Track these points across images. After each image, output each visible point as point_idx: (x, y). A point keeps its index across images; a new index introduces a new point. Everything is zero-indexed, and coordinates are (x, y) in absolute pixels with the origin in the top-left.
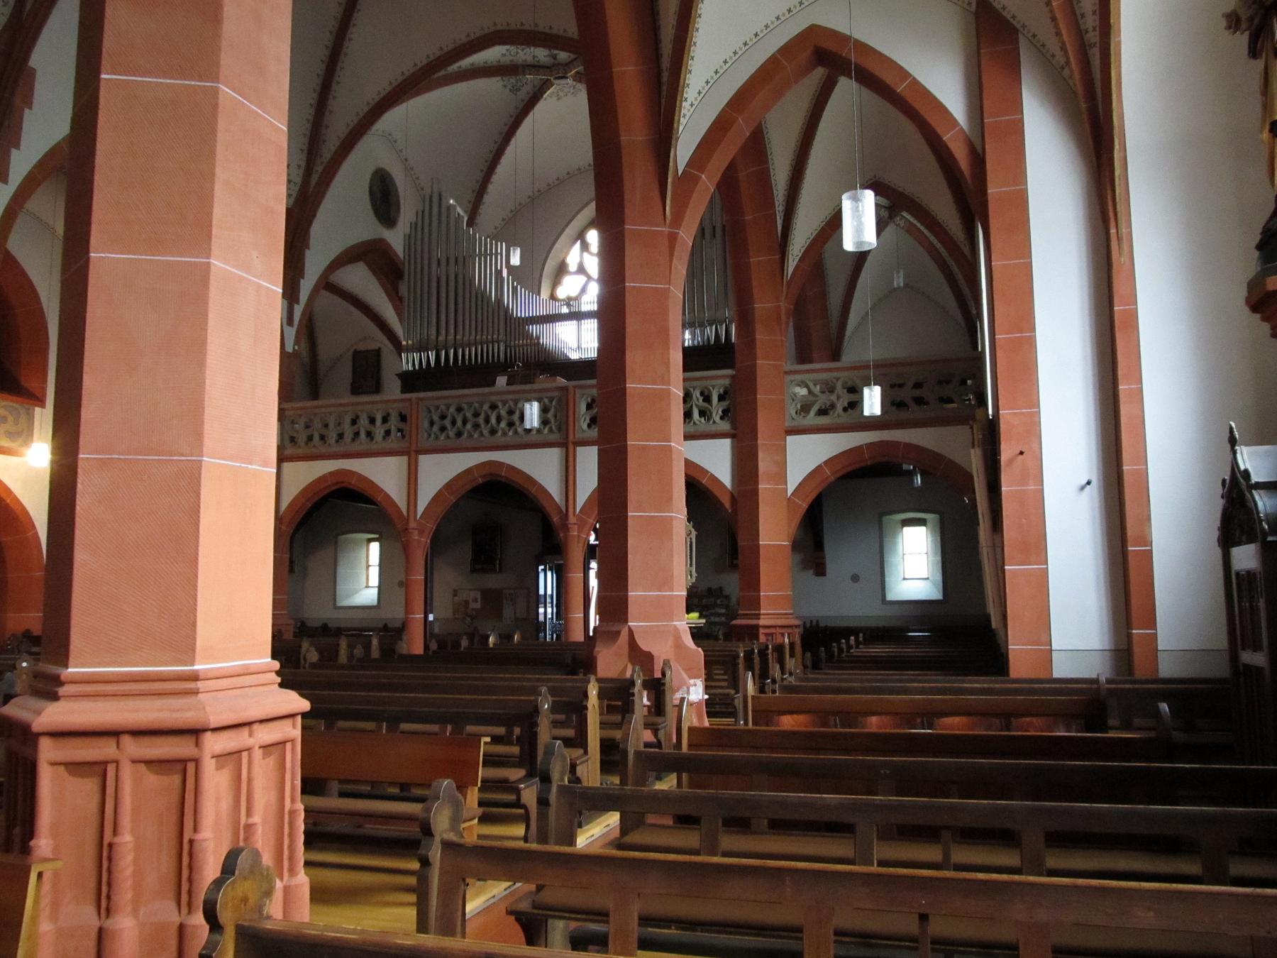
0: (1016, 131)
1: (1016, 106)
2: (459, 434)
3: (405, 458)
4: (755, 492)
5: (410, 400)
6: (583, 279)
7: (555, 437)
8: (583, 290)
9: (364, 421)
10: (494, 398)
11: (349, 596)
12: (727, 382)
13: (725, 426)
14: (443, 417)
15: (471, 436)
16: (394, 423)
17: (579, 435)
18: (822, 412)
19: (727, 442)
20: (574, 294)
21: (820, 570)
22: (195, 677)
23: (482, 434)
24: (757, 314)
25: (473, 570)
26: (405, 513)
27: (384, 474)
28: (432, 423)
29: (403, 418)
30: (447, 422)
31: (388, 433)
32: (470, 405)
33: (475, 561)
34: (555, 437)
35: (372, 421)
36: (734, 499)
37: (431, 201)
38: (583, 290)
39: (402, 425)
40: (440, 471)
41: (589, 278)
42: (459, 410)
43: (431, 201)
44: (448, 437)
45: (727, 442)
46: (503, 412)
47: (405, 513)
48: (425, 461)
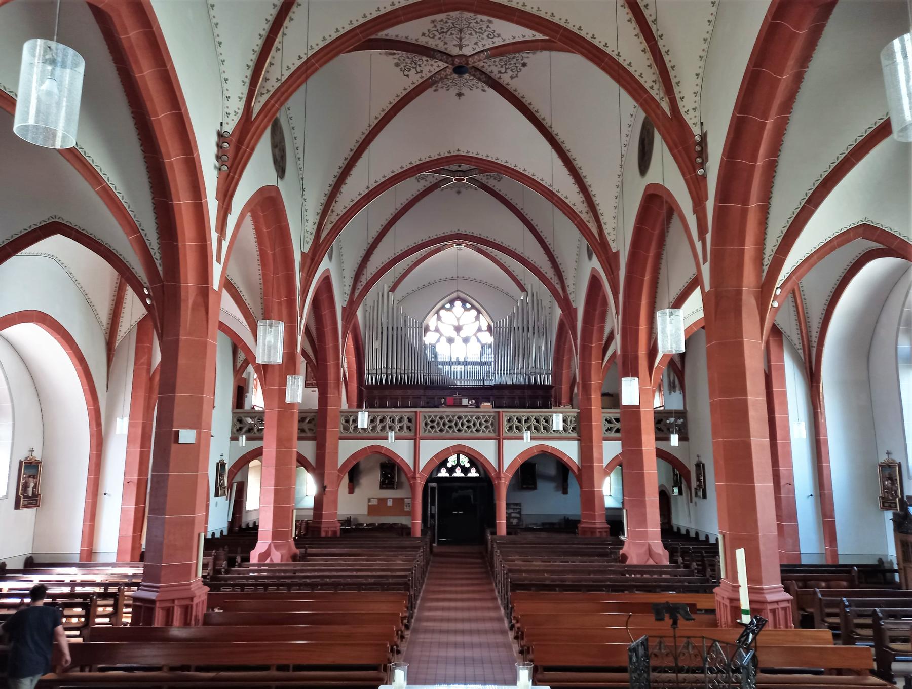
0: (782, 369)
1: (782, 360)
2: (441, 430)
3: (413, 441)
4: (592, 467)
5: (416, 412)
6: (437, 335)
7: (493, 435)
8: (438, 341)
9: (388, 420)
10: (460, 414)
11: (299, 502)
12: (575, 415)
13: (574, 435)
14: (432, 421)
15: (448, 431)
16: (405, 422)
17: (504, 435)
18: (618, 431)
19: (575, 443)
20: (433, 342)
21: (565, 492)
22: (762, 589)
23: (454, 431)
24: (593, 387)
25: (381, 488)
26: (412, 467)
27: (401, 449)
28: (426, 424)
29: (410, 420)
30: (435, 424)
31: (401, 428)
32: (448, 416)
33: (382, 483)
34: (493, 435)
35: (393, 421)
36: (579, 469)
37: (383, 296)
38: (438, 341)
39: (409, 424)
40: (430, 449)
41: (441, 335)
42: (441, 418)
43: (383, 296)
44: (435, 431)
45: (576, 442)
46: (465, 421)
47: (412, 467)
48: (423, 443)
